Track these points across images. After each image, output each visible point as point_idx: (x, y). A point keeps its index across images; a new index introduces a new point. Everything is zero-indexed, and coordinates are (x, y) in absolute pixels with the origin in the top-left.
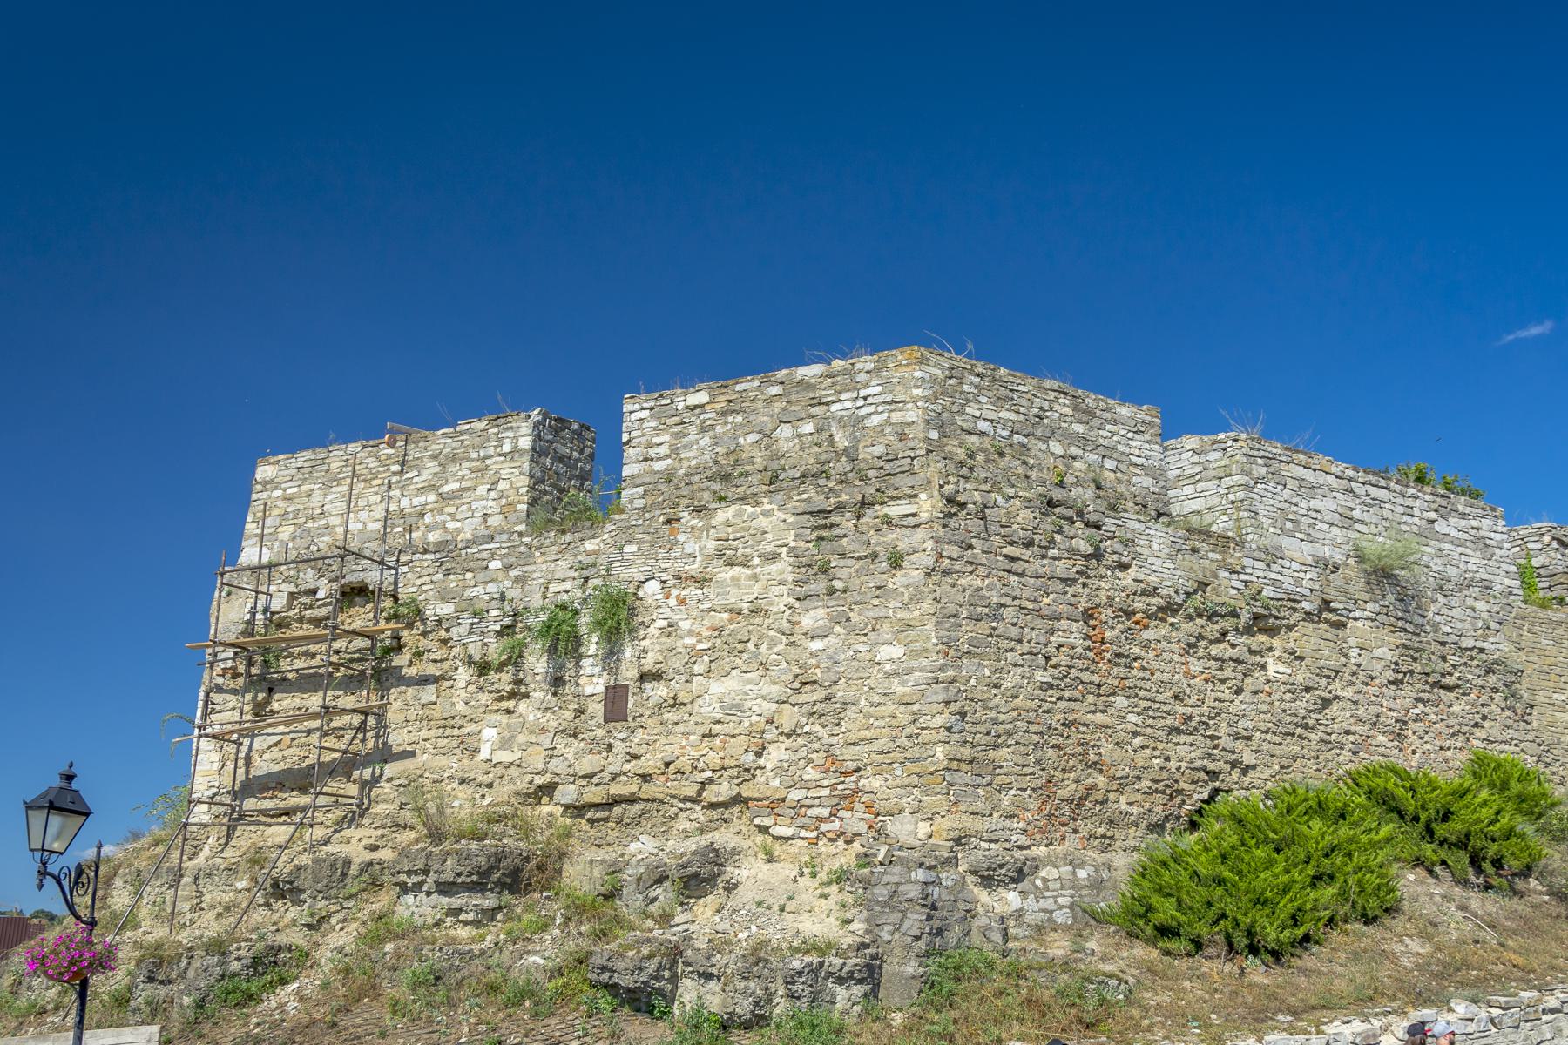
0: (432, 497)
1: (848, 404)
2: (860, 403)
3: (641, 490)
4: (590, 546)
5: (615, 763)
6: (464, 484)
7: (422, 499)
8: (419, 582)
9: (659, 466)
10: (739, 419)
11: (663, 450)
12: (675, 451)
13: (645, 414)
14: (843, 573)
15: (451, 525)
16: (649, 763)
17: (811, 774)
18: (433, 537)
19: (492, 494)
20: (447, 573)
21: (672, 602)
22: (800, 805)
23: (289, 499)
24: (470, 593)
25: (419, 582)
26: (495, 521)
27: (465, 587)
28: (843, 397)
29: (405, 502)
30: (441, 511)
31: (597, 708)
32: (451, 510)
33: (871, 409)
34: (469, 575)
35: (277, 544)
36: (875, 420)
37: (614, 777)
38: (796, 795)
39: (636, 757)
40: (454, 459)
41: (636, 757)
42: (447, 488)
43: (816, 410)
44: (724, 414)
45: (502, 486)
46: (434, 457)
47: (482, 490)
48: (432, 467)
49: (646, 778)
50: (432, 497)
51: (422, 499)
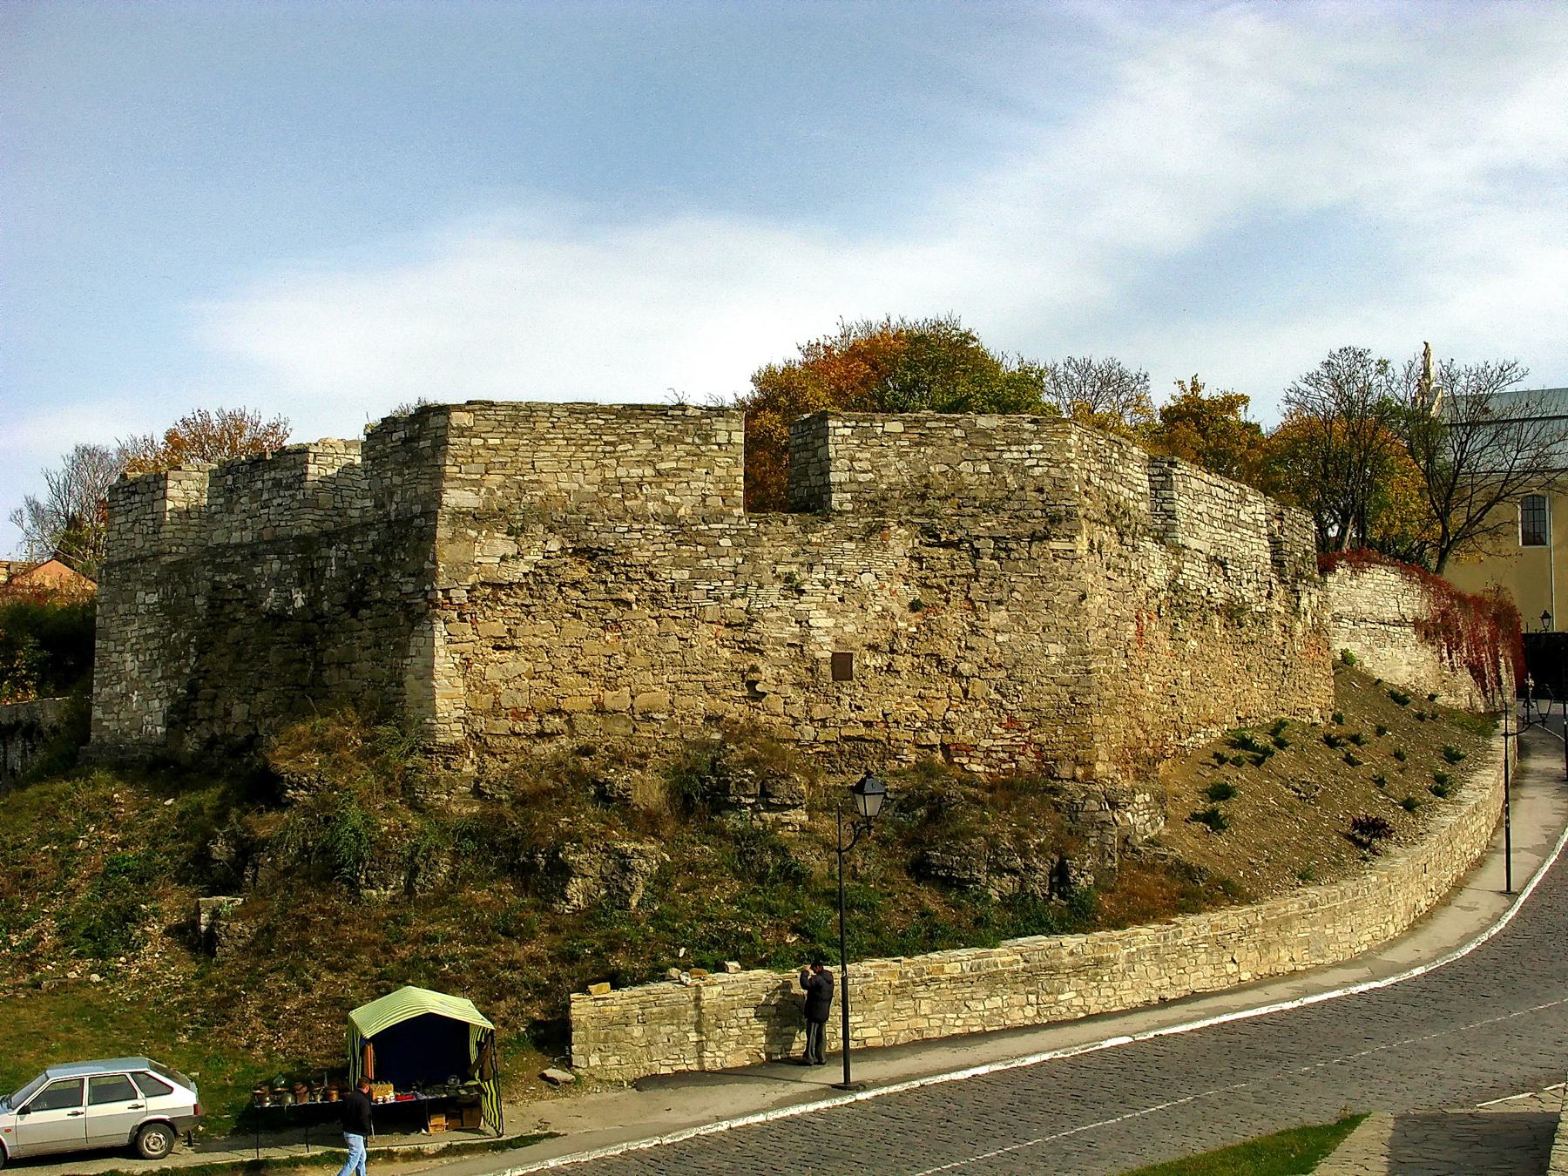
0: (649, 472)
1: (1016, 455)
2: (1026, 455)
3: (849, 496)
5: (845, 712)
6: (681, 465)
7: (636, 472)
8: (652, 548)
9: (861, 477)
10: (929, 451)
11: (866, 465)
12: (874, 468)
13: (848, 432)
14: (1021, 587)
15: (669, 498)
17: (996, 730)
19: (710, 478)
20: (680, 543)
21: (887, 593)
22: (988, 751)
23: (495, 449)
24: (705, 563)
25: (652, 548)
26: (715, 502)
27: (698, 559)
28: (1014, 448)
29: (621, 472)
30: (659, 485)
31: (826, 668)
32: (672, 486)
33: (1034, 462)
34: (701, 548)
35: (483, 490)
36: (1037, 471)
37: (845, 722)
38: (986, 743)
39: (859, 708)
40: (668, 441)
41: (859, 708)
42: (662, 466)
43: (991, 455)
44: (917, 444)
45: (718, 472)
46: (648, 434)
48: (645, 444)
49: (868, 724)
50: (649, 472)
51: (636, 472)
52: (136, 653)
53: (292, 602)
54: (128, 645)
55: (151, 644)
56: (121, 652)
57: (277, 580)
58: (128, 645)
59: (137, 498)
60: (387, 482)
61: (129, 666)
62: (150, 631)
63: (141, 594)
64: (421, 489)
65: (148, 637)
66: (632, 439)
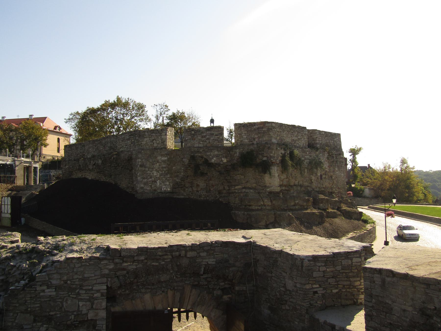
4: (317, 153)
9: (320, 142)
16: (324, 186)
18: (297, 145)
31: (319, 177)
42: (299, 137)
47: (303, 139)
52: (157, 171)
53: (222, 161)
54: (155, 169)
55: (165, 169)
56: (151, 171)
57: (217, 156)
58: (155, 169)
59: (154, 134)
60: (253, 136)
61: (155, 174)
62: (163, 166)
63: (159, 158)
64: (264, 139)
65: (163, 168)
66: (294, 132)
